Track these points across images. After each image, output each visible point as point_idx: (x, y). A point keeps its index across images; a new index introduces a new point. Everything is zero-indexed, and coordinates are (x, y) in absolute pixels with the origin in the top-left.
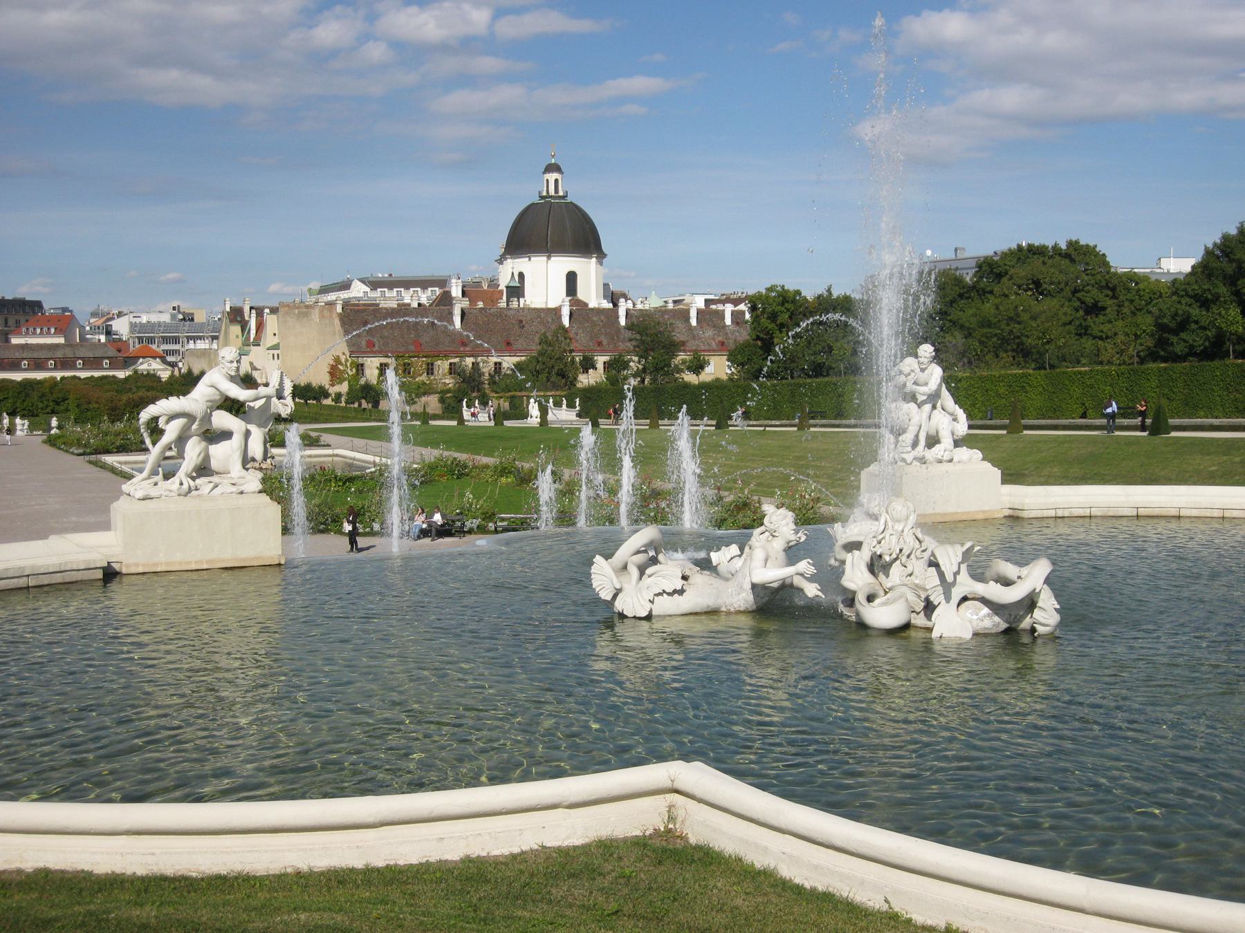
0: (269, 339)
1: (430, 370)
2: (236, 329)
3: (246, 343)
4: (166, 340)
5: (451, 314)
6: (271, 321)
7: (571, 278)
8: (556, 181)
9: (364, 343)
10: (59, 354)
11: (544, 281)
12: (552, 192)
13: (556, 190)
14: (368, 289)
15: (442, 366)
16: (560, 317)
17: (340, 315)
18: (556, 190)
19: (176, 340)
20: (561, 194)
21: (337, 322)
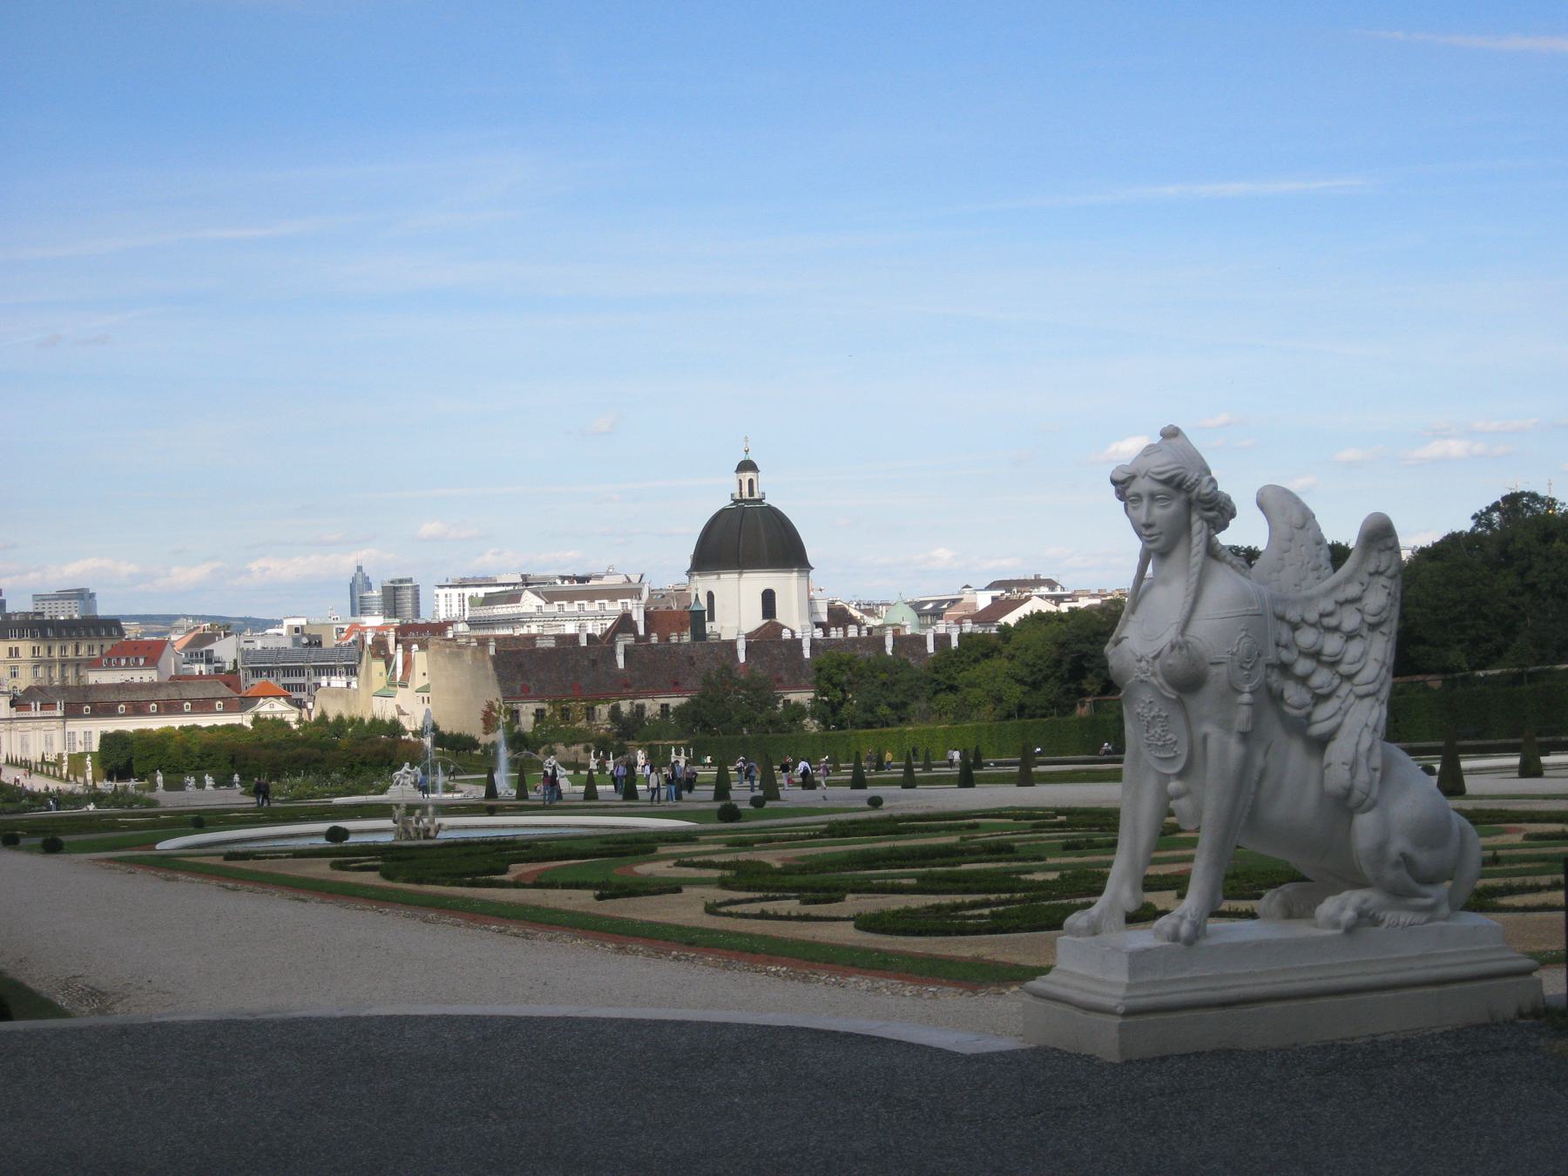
0: (418, 680)
1: (590, 714)
2: (379, 666)
3: (392, 683)
4: (288, 671)
5: (613, 652)
6: (420, 658)
7: (768, 598)
8: (751, 482)
9: (518, 687)
10: (162, 695)
11: (735, 604)
12: (746, 495)
13: (751, 492)
14: (542, 603)
15: (603, 710)
16: (736, 651)
17: (492, 657)
18: (751, 492)
19: (300, 671)
20: (756, 496)
21: (490, 665)
